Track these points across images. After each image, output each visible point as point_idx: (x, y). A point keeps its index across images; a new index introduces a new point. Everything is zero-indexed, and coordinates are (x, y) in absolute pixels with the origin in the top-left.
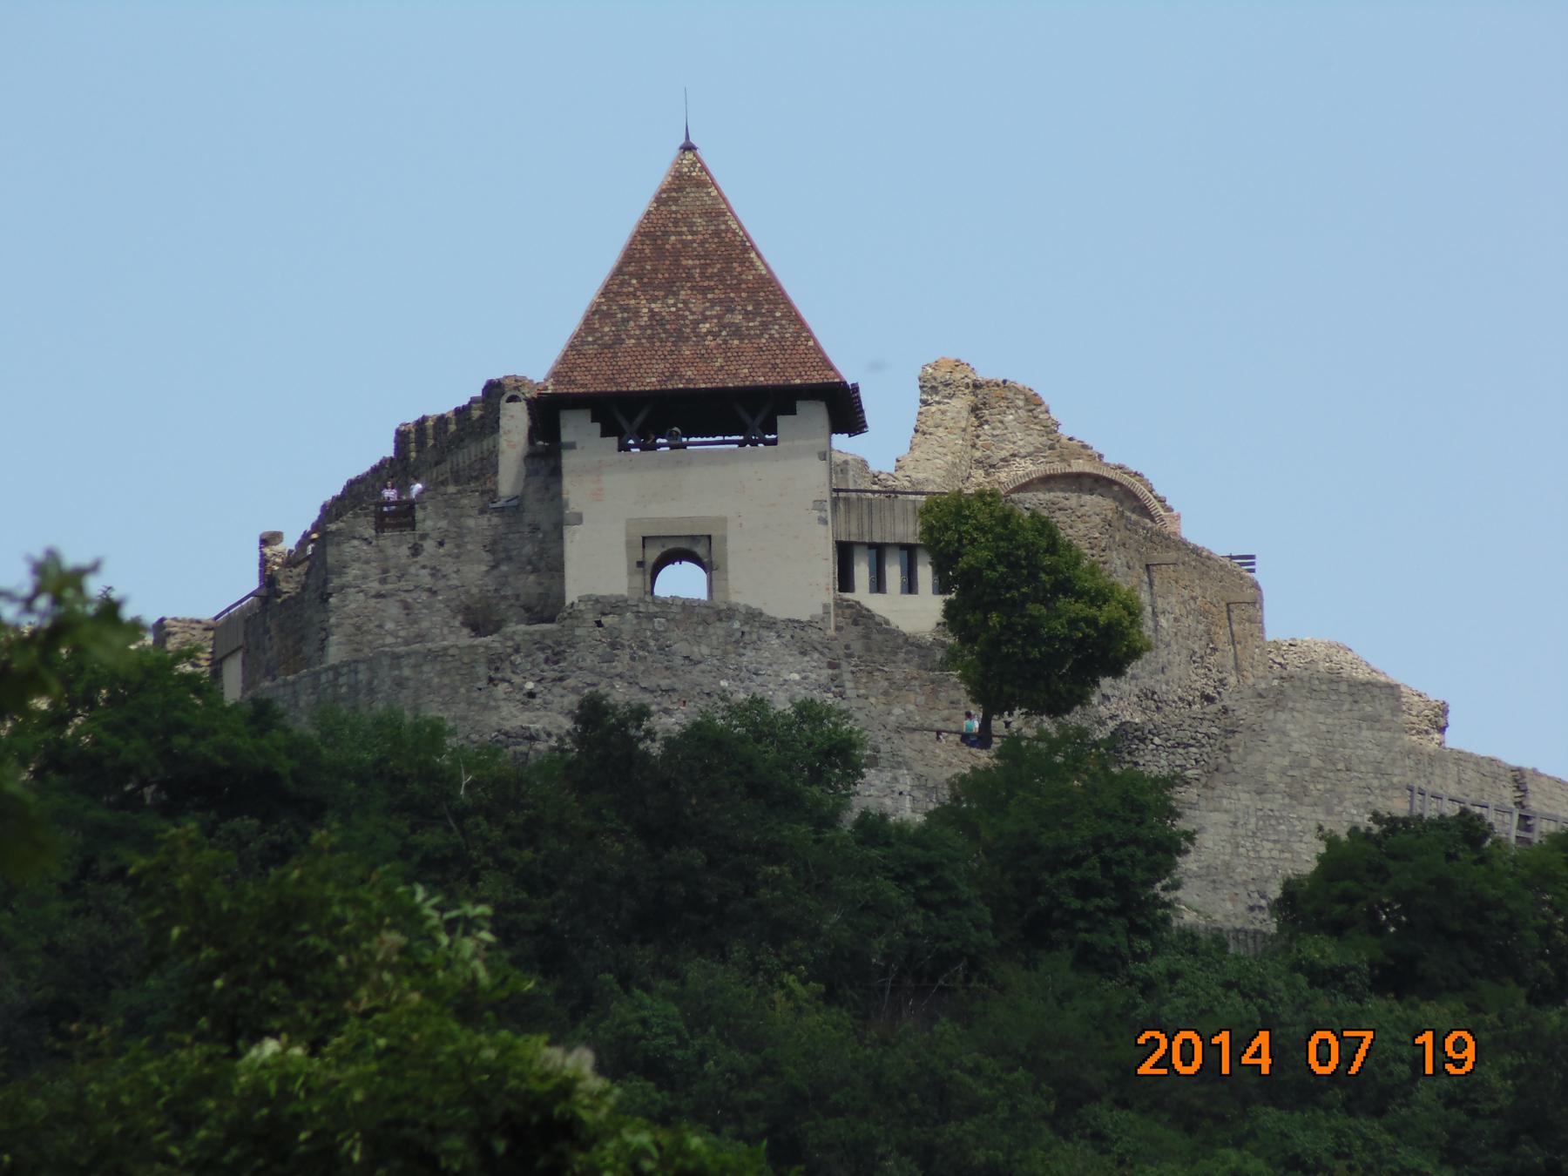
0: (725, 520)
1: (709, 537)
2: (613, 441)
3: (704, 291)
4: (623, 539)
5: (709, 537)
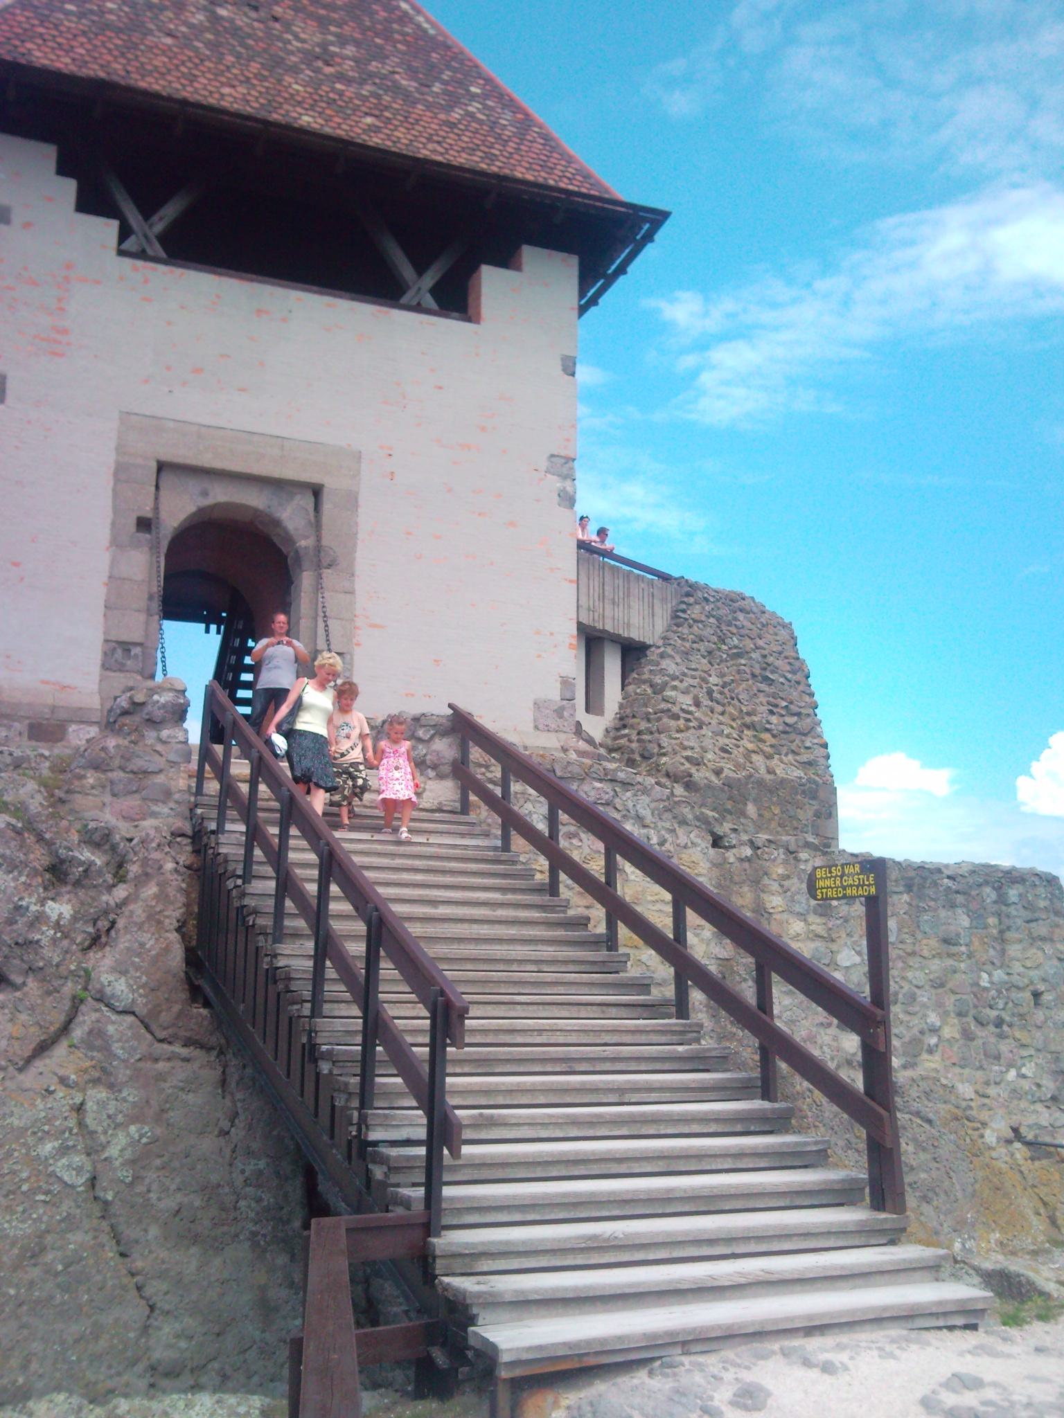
0: (358, 457)
1: (316, 491)
2: (110, 228)
3: (323, 23)
4: (111, 459)
5: (316, 491)
